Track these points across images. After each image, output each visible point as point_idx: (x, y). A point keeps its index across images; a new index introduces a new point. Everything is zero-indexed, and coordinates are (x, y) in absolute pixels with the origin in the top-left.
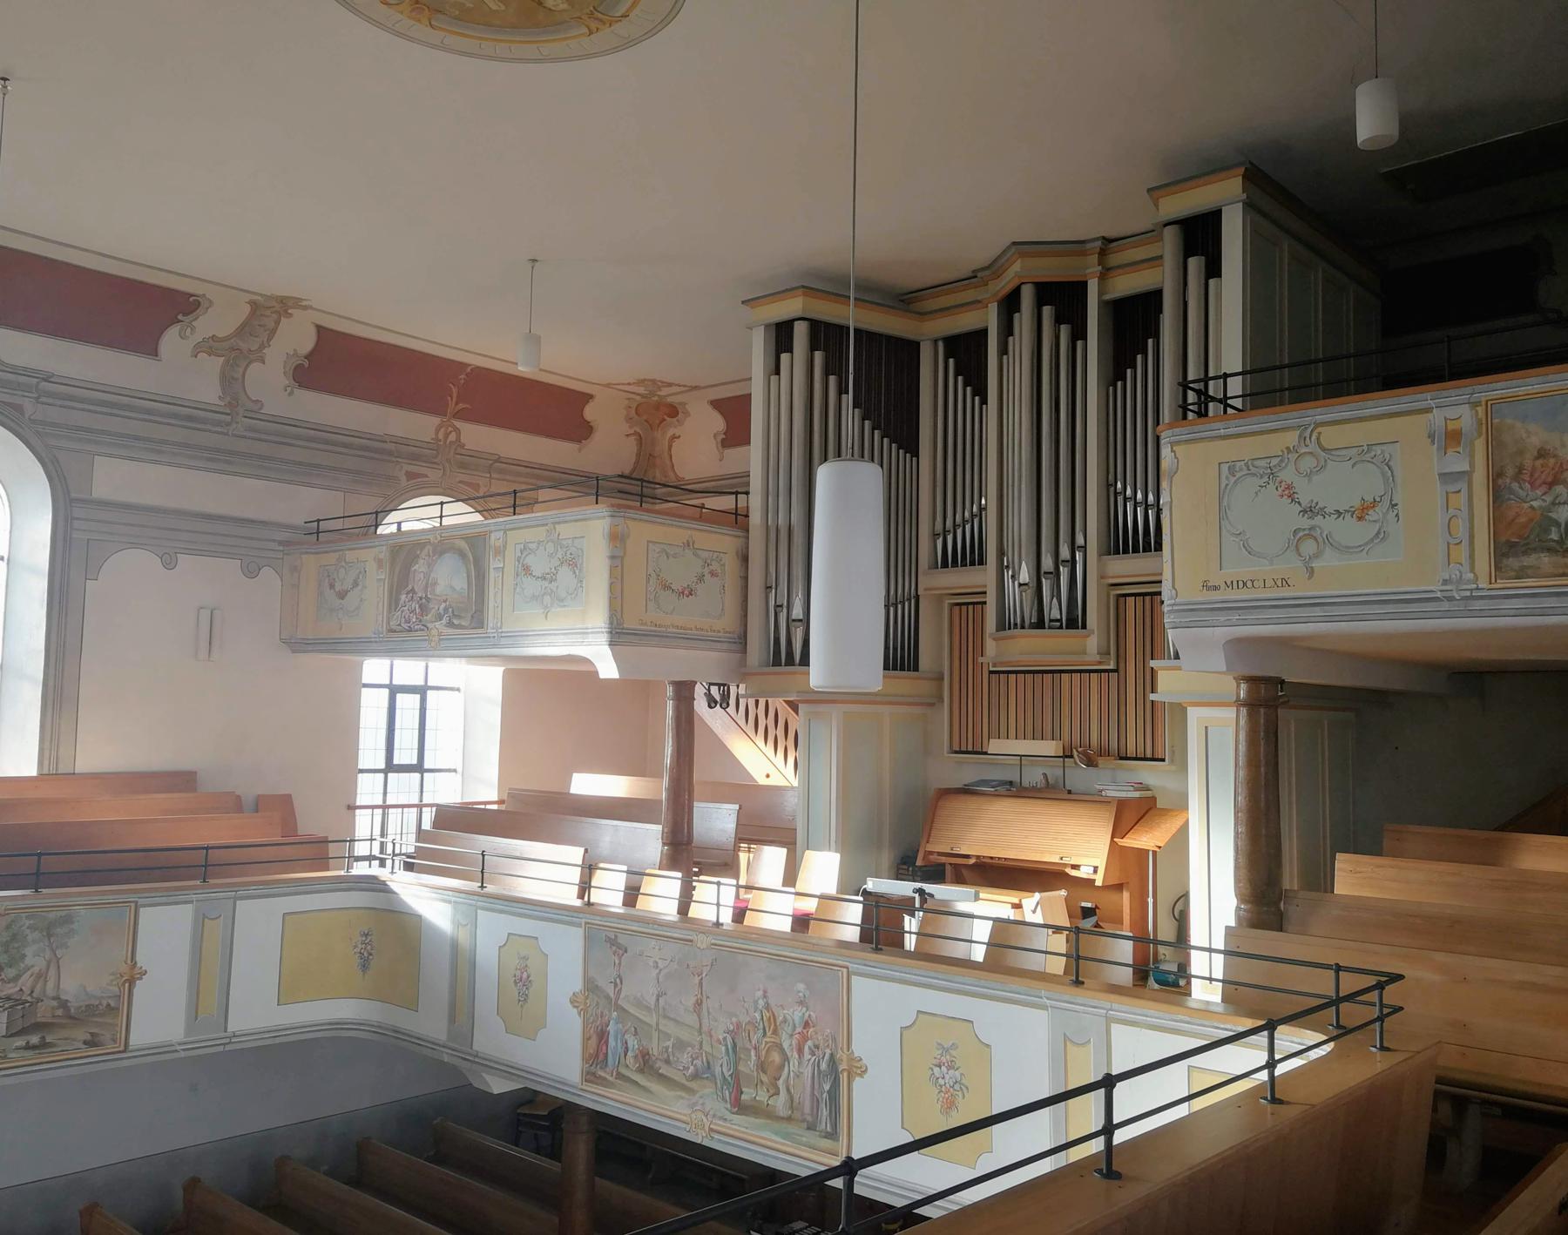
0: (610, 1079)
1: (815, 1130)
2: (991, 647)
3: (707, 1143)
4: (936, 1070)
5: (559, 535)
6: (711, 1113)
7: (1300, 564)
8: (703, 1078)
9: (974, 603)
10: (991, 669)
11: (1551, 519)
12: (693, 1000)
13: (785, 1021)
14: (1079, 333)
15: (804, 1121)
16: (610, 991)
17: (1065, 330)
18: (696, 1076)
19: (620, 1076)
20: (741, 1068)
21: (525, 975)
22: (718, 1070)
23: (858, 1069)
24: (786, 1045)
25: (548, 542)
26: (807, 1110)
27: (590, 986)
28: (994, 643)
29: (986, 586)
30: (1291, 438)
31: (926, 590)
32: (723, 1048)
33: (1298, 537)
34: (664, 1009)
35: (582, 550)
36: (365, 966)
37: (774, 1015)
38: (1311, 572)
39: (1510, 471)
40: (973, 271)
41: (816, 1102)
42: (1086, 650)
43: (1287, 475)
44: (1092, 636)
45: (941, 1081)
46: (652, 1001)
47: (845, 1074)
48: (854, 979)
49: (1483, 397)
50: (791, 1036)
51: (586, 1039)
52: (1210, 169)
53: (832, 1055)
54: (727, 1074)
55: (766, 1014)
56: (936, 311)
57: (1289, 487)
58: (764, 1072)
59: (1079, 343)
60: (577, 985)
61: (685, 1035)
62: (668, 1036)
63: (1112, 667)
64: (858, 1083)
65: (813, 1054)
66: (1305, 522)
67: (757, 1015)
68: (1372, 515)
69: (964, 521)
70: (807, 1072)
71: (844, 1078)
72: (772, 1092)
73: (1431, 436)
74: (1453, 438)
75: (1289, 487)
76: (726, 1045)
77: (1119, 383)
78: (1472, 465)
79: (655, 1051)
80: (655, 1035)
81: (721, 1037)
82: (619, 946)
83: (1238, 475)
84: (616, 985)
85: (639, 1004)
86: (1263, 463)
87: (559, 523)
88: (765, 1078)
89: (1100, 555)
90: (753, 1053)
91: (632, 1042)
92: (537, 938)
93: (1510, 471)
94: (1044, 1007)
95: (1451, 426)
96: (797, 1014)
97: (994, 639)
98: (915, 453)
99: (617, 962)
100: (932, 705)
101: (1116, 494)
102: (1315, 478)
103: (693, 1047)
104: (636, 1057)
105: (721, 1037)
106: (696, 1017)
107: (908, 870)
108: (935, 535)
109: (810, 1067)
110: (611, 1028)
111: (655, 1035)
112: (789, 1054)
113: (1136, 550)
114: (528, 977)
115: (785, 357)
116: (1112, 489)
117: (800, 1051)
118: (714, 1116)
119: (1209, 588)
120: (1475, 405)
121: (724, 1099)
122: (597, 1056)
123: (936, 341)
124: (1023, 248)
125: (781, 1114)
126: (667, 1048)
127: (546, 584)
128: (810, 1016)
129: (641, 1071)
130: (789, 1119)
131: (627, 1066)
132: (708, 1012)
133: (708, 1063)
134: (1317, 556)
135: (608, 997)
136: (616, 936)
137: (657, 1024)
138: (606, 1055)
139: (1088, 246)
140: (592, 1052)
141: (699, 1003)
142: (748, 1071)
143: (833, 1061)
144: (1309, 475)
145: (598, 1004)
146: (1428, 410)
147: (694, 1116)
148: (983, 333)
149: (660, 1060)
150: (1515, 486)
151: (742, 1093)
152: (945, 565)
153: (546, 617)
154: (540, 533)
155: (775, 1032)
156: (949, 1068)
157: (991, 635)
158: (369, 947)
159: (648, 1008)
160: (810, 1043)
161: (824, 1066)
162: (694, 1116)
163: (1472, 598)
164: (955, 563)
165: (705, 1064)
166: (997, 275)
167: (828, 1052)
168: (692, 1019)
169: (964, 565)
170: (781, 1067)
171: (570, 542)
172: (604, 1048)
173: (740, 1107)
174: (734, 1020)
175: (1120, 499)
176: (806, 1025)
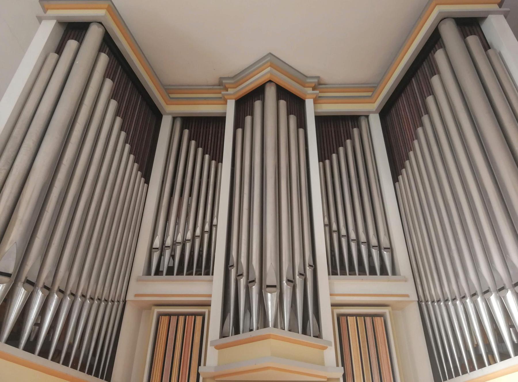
9: (185, 315)
14: (302, 124)
17: (293, 119)
28: (217, 351)
29: (210, 296)
31: (136, 295)
40: (221, 79)
42: (323, 359)
44: (329, 347)
77: (327, 162)
97: (218, 347)
98: (147, 182)
123: (174, 119)
139: (309, 80)
166: (237, 84)
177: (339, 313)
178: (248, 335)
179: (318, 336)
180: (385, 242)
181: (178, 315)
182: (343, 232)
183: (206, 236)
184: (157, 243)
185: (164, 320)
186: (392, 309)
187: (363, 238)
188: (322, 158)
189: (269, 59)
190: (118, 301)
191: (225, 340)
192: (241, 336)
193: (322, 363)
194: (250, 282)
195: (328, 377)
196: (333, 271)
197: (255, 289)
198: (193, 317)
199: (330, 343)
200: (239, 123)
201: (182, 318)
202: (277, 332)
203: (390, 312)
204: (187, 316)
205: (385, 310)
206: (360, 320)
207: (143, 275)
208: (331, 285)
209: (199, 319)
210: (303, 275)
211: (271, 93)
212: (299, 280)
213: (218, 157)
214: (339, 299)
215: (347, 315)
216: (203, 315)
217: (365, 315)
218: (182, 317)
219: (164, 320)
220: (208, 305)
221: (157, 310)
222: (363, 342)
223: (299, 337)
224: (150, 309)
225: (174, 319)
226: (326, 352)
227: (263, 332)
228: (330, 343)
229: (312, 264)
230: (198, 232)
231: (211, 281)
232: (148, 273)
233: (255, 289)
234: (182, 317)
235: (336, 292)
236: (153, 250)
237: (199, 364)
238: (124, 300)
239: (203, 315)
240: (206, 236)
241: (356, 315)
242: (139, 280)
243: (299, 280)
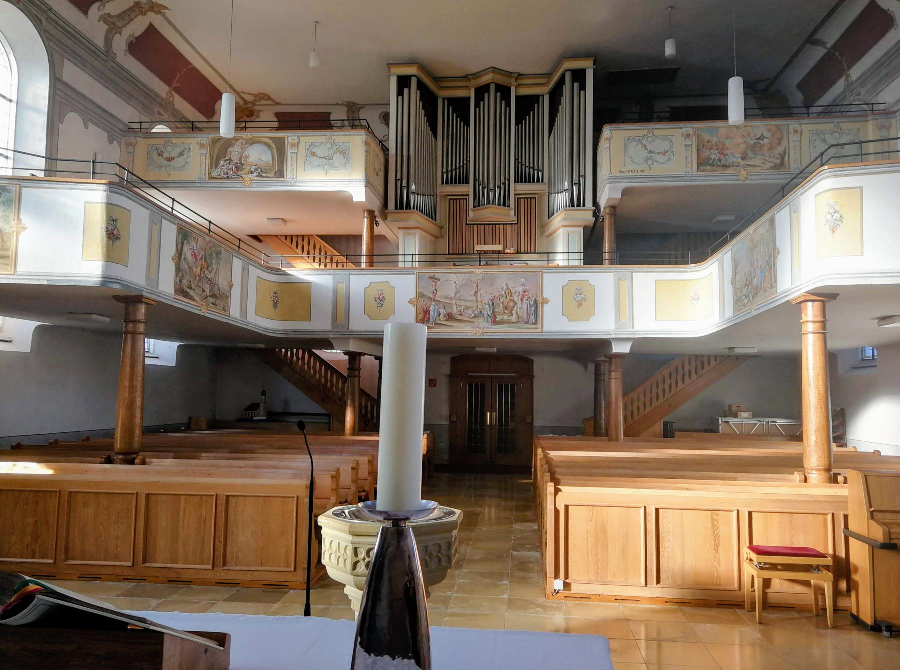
0: (431, 326)
1: (529, 323)
2: (471, 214)
3: (481, 337)
4: (576, 297)
5: (334, 141)
6: (483, 327)
7: (648, 167)
8: (478, 317)
9: (460, 199)
10: (468, 223)
11: (710, 158)
12: (474, 292)
13: (516, 292)
14: (508, 105)
15: (524, 322)
16: (432, 296)
18: (475, 317)
19: (436, 324)
20: (496, 310)
21: (381, 297)
22: (485, 313)
23: (546, 301)
24: (516, 300)
25: (327, 143)
26: (525, 318)
27: (420, 295)
30: (646, 132)
31: (440, 192)
32: (488, 306)
33: (647, 159)
34: (459, 297)
35: (349, 148)
36: (275, 306)
37: (511, 291)
38: (651, 169)
39: (701, 146)
40: (467, 75)
41: (529, 315)
43: (645, 142)
45: (577, 299)
46: (453, 295)
47: (541, 304)
48: (544, 275)
49: (696, 126)
50: (518, 296)
51: (417, 315)
52: (586, 56)
53: (535, 300)
54: (489, 314)
55: (507, 291)
56: (447, 87)
57: (645, 145)
58: (507, 310)
59: (508, 109)
60: (412, 294)
61: (469, 305)
62: (461, 306)
63: (516, 222)
64: (546, 306)
65: (527, 300)
66: (649, 155)
67: (504, 292)
68: (667, 154)
70: (525, 306)
71: (540, 306)
72: (510, 316)
73: (683, 135)
74: (688, 136)
75: (645, 145)
76: (489, 305)
77: (520, 125)
78: (693, 143)
79: (454, 311)
80: (455, 307)
81: (487, 302)
82: (436, 279)
83: (631, 141)
84: (434, 293)
85: (446, 298)
86: (637, 138)
87: (334, 136)
88: (507, 312)
89: (515, 182)
90: (501, 305)
91: (442, 311)
92: (389, 282)
93: (701, 146)
94: (613, 272)
95: (688, 133)
96: (521, 289)
97: (473, 211)
99: (434, 284)
101: (519, 163)
102: (652, 143)
103: (473, 308)
104: (445, 316)
105: (487, 302)
106: (475, 297)
108: (443, 173)
109: (526, 306)
110: (432, 308)
111: (455, 307)
112: (517, 302)
113: (526, 182)
114: (384, 297)
115: (406, 91)
116: (517, 161)
117: (522, 300)
118: (484, 328)
119: (621, 172)
120: (693, 128)
121: (489, 322)
122: (424, 319)
123: (444, 99)
124: (495, 70)
125: (514, 321)
126: (461, 311)
127: (327, 160)
128: (526, 289)
129: (447, 320)
130: (518, 322)
131: (440, 320)
132: (481, 295)
133: (481, 312)
134: (653, 164)
135: (430, 298)
136: (434, 276)
137: (456, 303)
138: (429, 318)
139: (513, 75)
140: (421, 318)
141: (476, 293)
142: (499, 311)
143: (536, 301)
144: (651, 143)
145: (424, 301)
146: (682, 128)
147: (474, 330)
148: (469, 99)
149: (457, 315)
150: (702, 149)
151: (497, 318)
153: (326, 175)
154: (324, 139)
155: (511, 296)
156: (580, 295)
157: (471, 209)
158: (277, 299)
159: (451, 299)
160: (526, 297)
161: (532, 303)
162: (474, 330)
163: (692, 176)
164: (452, 183)
165: (480, 312)
167: (534, 299)
168: (474, 299)
169: (460, 183)
170: (515, 307)
171: (342, 144)
172: (428, 316)
173: (495, 323)
174: (493, 296)
175: (520, 165)
176: (525, 292)
178: (484, 207)
179: (509, 206)
180: (541, 168)
181: (457, 199)
182: (524, 163)
183: (465, 166)
184: (445, 170)
185: (452, 201)
187: (532, 166)
188: (517, 124)
189: (491, 70)
191: (475, 209)
192: (481, 207)
194: (484, 188)
196: (517, 181)
197: (486, 191)
199: (513, 209)
200: (477, 106)
201: (458, 201)
202: (494, 206)
208: (515, 187)
209: (465, 201)
210: (505, 184)
211: (493, 88)
212: (503, 187)
213: (469, 126)
214: (518, 193)
215: (521, 198)
216: (466, 199)
217: (528, 198)
219: (452, 201)
220: (469, 195)
223: (502, 207)
225: (455, 201)
226: (511, 212)
227: (489, 206)
228: (513, 209)
230: (462, 165)
231: (469, 186)
232: (443, 183)
233: (486, 191)
239: (466, 199)
240: (465, 166)
241: (525, 198)
242: (440, 186)
243: (503, 187)
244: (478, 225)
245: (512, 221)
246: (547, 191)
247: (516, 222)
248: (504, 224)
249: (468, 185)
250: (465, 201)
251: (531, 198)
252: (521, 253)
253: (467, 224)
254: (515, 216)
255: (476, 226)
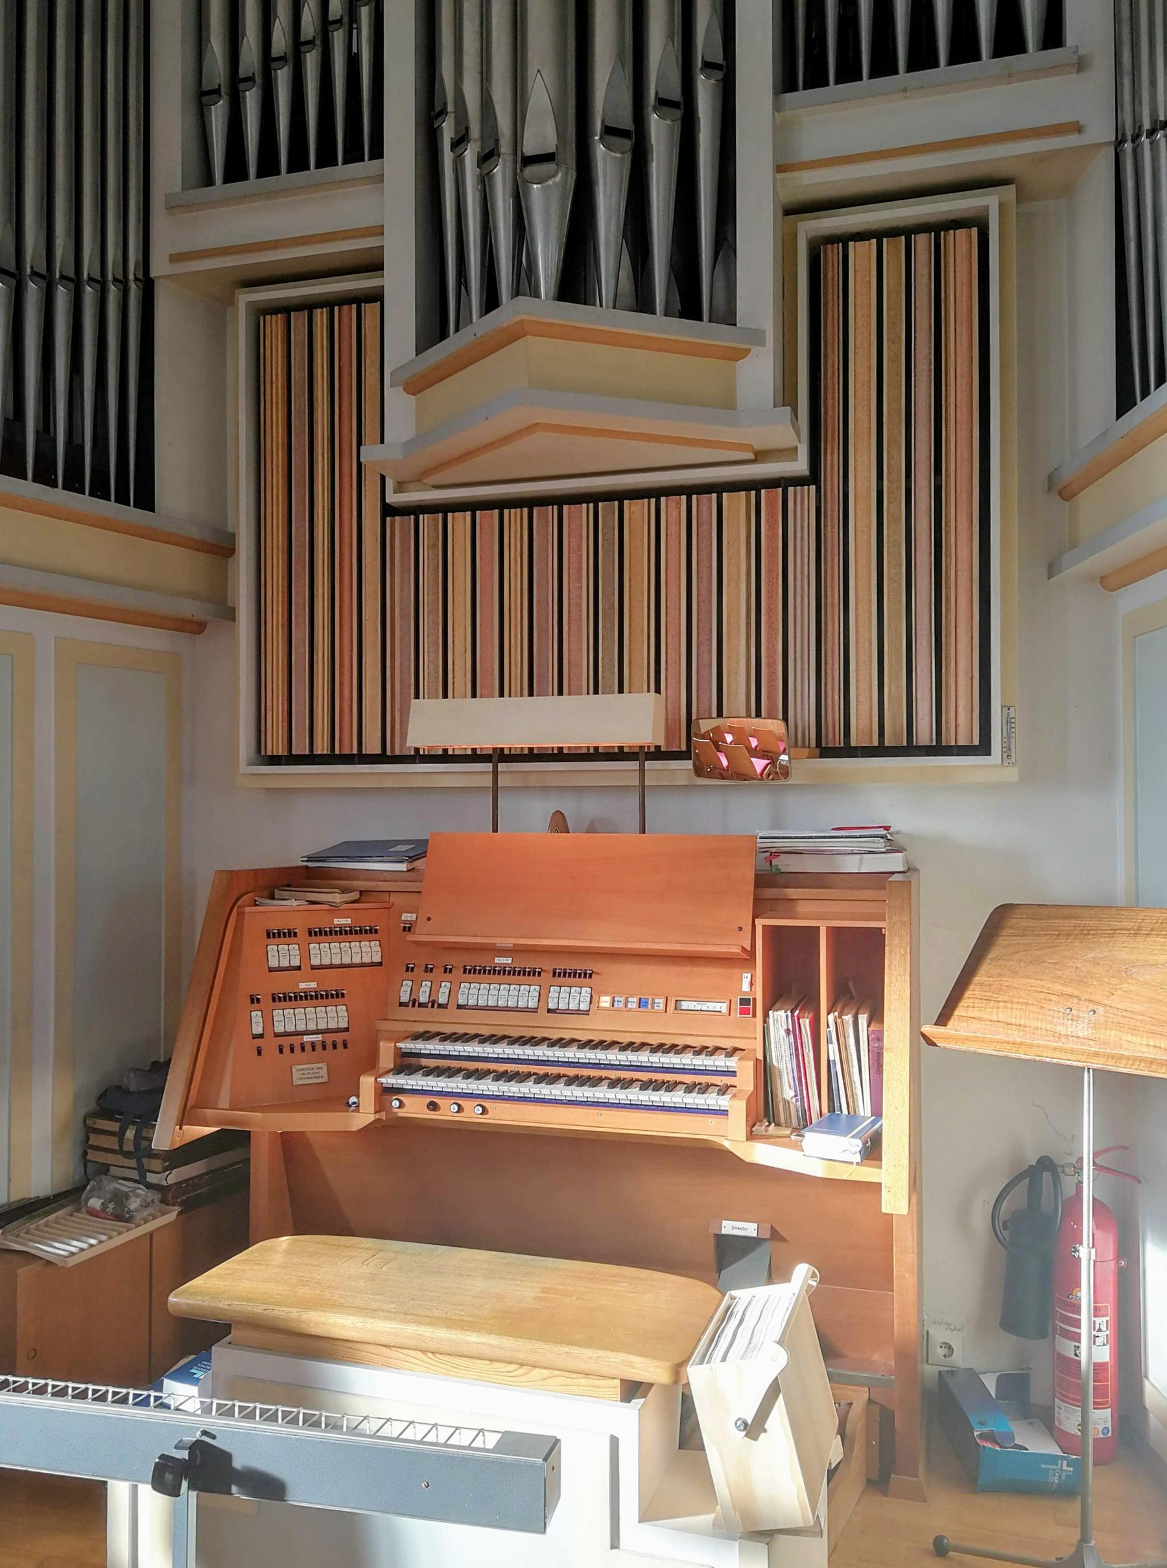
10: (392, 498)
31: (175, 258)
69: (298, 45)
89: (787, 82)
97: (416, 386)
100: (197, 627)
107: (121, 1135)
108: (202, 97)
152: (235, 171)
177: (814, 234)
186: (1022, 197)
190: (123, 283)
193: (727, 402)
195: (758, 446)
198: (354, 306)
199: (757, 337)
201: (321, 316)
203: (1002, 206)
204: (336, 308)
205: (988, 201)
206: (894, 249)
207: (185, 188)
208: (782, 133)
209: (370, 310)
218: (322, 313)
219: (275, 324)
221: (246, 298)
222: (893, 324)
224: (231, 302)
226: (742, 366)
228: (757, 337)
229: (718, 58)
231: (380, 178)
234: (322, 313)
235: (806, 157)
236: (205, 99)
237: (359, 443)
238: (141, 277)
241: (879, 235)
244: (473, 506)
245: (761, 456)
246: (1101, 130)
247: (800, 466)
248: (689, 491)
249: (366, 167)
250: (370, 310)
251: (938, 228)
252: (848, 751)
253: (388, 510)
254: (787, 397)
255: (460, 522)
